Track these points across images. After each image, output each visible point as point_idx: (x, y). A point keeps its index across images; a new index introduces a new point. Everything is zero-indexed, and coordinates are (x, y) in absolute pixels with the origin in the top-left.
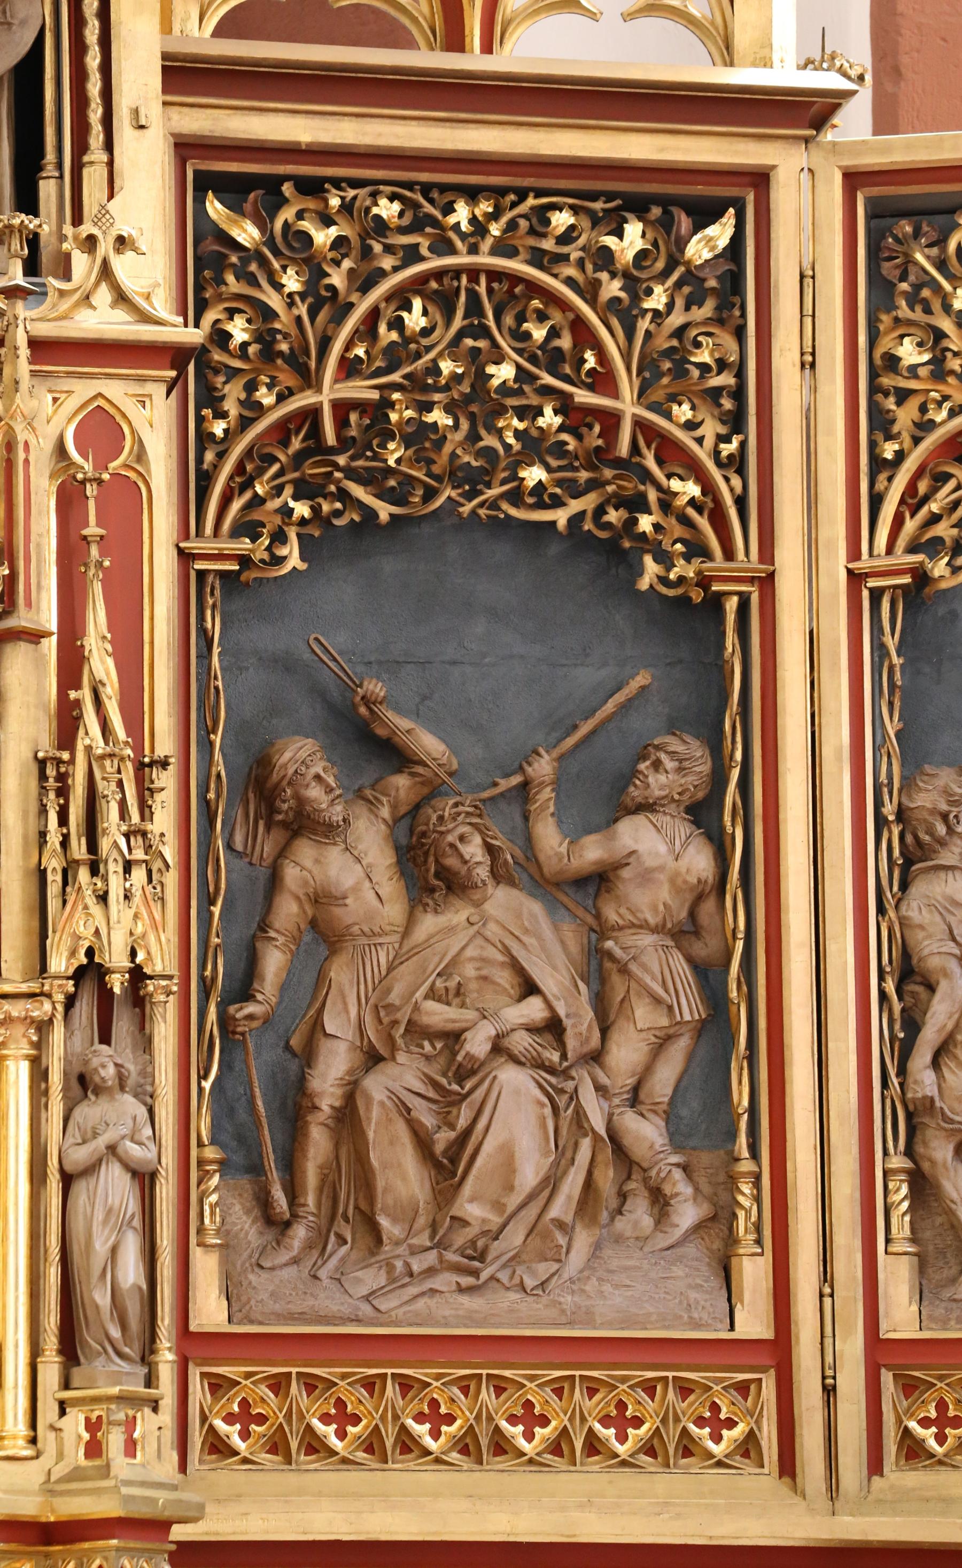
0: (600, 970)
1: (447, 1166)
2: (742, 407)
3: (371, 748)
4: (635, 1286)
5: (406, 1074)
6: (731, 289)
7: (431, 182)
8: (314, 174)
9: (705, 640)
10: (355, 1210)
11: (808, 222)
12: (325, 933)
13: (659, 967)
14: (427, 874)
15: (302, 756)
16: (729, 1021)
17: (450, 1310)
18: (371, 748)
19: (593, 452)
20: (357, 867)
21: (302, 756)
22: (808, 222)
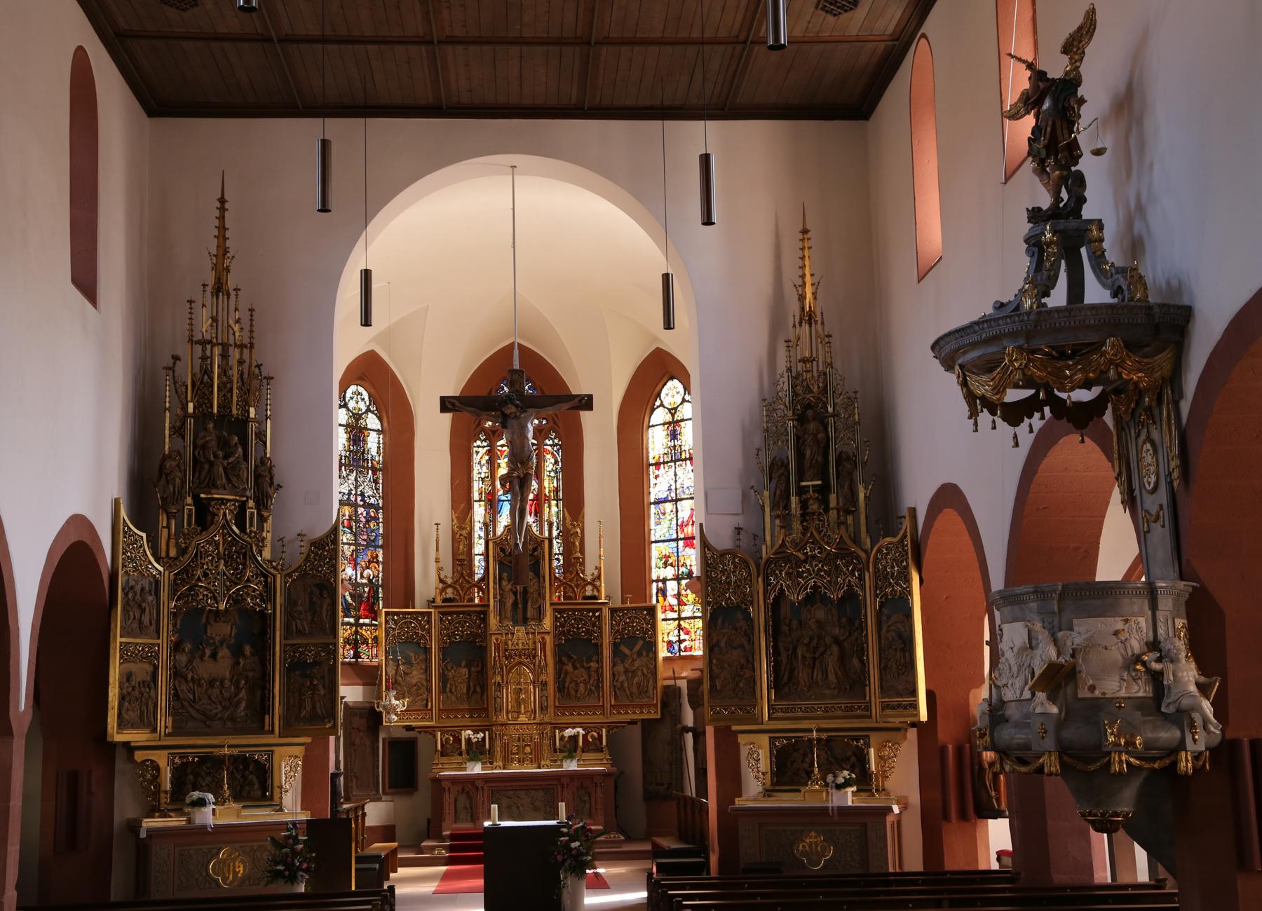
0: (589, 676)
1: (576, 691)
2: (600, 628)
3: (570, 658)
4: (592, 701)
5: (573, 685)
6: (599, 618)
7: (574, 611)
8: (564, 610)
9: (597, 648)
10: (569, 695)
11: (606, 612)
12: (567, 673)
13: (594, 675)
14: (575, 668)
15: (565, 659)
16: (600, 679)
17: (577, 704)
18: (570, 658)
19: (588, 632)
20: (569, 668)
21: (565, 659)
22: (606, 612)
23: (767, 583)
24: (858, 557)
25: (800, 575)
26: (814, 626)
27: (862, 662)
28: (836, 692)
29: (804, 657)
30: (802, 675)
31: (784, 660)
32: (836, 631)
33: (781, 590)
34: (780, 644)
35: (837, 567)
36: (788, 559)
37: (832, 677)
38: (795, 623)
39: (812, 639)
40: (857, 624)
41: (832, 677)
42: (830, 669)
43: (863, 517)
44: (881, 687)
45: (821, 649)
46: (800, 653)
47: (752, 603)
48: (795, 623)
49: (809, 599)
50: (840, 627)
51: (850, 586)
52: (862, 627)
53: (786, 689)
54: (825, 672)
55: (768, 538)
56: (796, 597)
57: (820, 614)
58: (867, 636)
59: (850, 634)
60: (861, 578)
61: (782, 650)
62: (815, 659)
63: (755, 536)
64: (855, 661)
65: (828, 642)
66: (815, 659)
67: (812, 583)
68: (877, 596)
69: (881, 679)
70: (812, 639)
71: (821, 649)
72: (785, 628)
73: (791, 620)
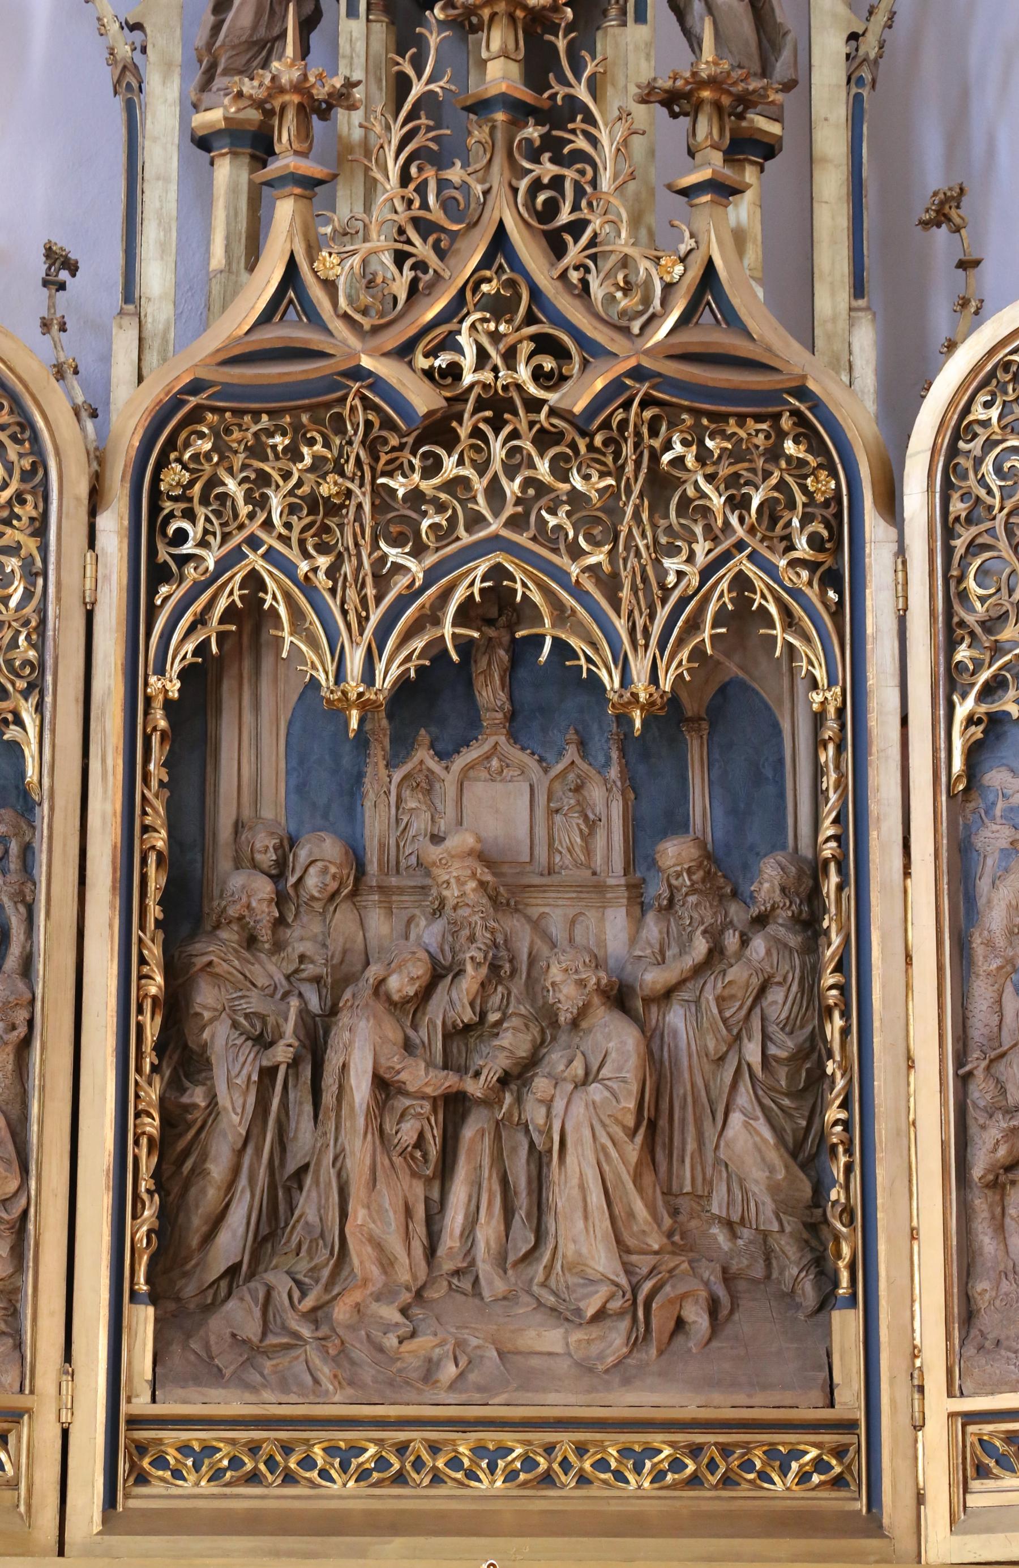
23: (152, 570)
24: (816, 425)
25: (397, 522)
26: (458, 882)
27: (807, 1151)
28: (615, 1338)
29: (384, 1086)
30: (378, 1219)
31: (235, 1109)
32: (613, 929)
33: (251, 618)
34: (206, 997)
35: (661, 484)
36: (321, 402)
37: (584, 1240)
38: (320, 859)
39: (440, 973)
40: (769, 880)
41: (584, 1240)
42: (577, 1183)
43: (831, 185)
44: (965, 1314)
45: (512, 1042)
46: (360, 1049)
47: (35, 687)
48: (320, 859)
49: (429, 704)
50: (638, 901)
51: (743, 617)
52: (818, 908)
53: (240, 1315)
54: (528, 1202)
55: (156, 277)
56: (358, 666)
57: (493, 801)
58: (856, 962)
59: (716, 953)
60: (838, 569)
61: (218, 1037)
62: (454, 1107)
63: (60, 264)
64: (750, 1140)
65: (567, 997)
66: (454, 1107)
67: (472, 581)
68: (951, 680)
69: (965, 1262)
70: (440, 973)
71: (512, 1042)
72: (250, 892)
73: (289, 844)
